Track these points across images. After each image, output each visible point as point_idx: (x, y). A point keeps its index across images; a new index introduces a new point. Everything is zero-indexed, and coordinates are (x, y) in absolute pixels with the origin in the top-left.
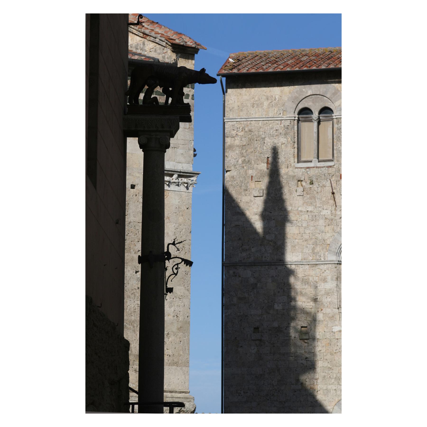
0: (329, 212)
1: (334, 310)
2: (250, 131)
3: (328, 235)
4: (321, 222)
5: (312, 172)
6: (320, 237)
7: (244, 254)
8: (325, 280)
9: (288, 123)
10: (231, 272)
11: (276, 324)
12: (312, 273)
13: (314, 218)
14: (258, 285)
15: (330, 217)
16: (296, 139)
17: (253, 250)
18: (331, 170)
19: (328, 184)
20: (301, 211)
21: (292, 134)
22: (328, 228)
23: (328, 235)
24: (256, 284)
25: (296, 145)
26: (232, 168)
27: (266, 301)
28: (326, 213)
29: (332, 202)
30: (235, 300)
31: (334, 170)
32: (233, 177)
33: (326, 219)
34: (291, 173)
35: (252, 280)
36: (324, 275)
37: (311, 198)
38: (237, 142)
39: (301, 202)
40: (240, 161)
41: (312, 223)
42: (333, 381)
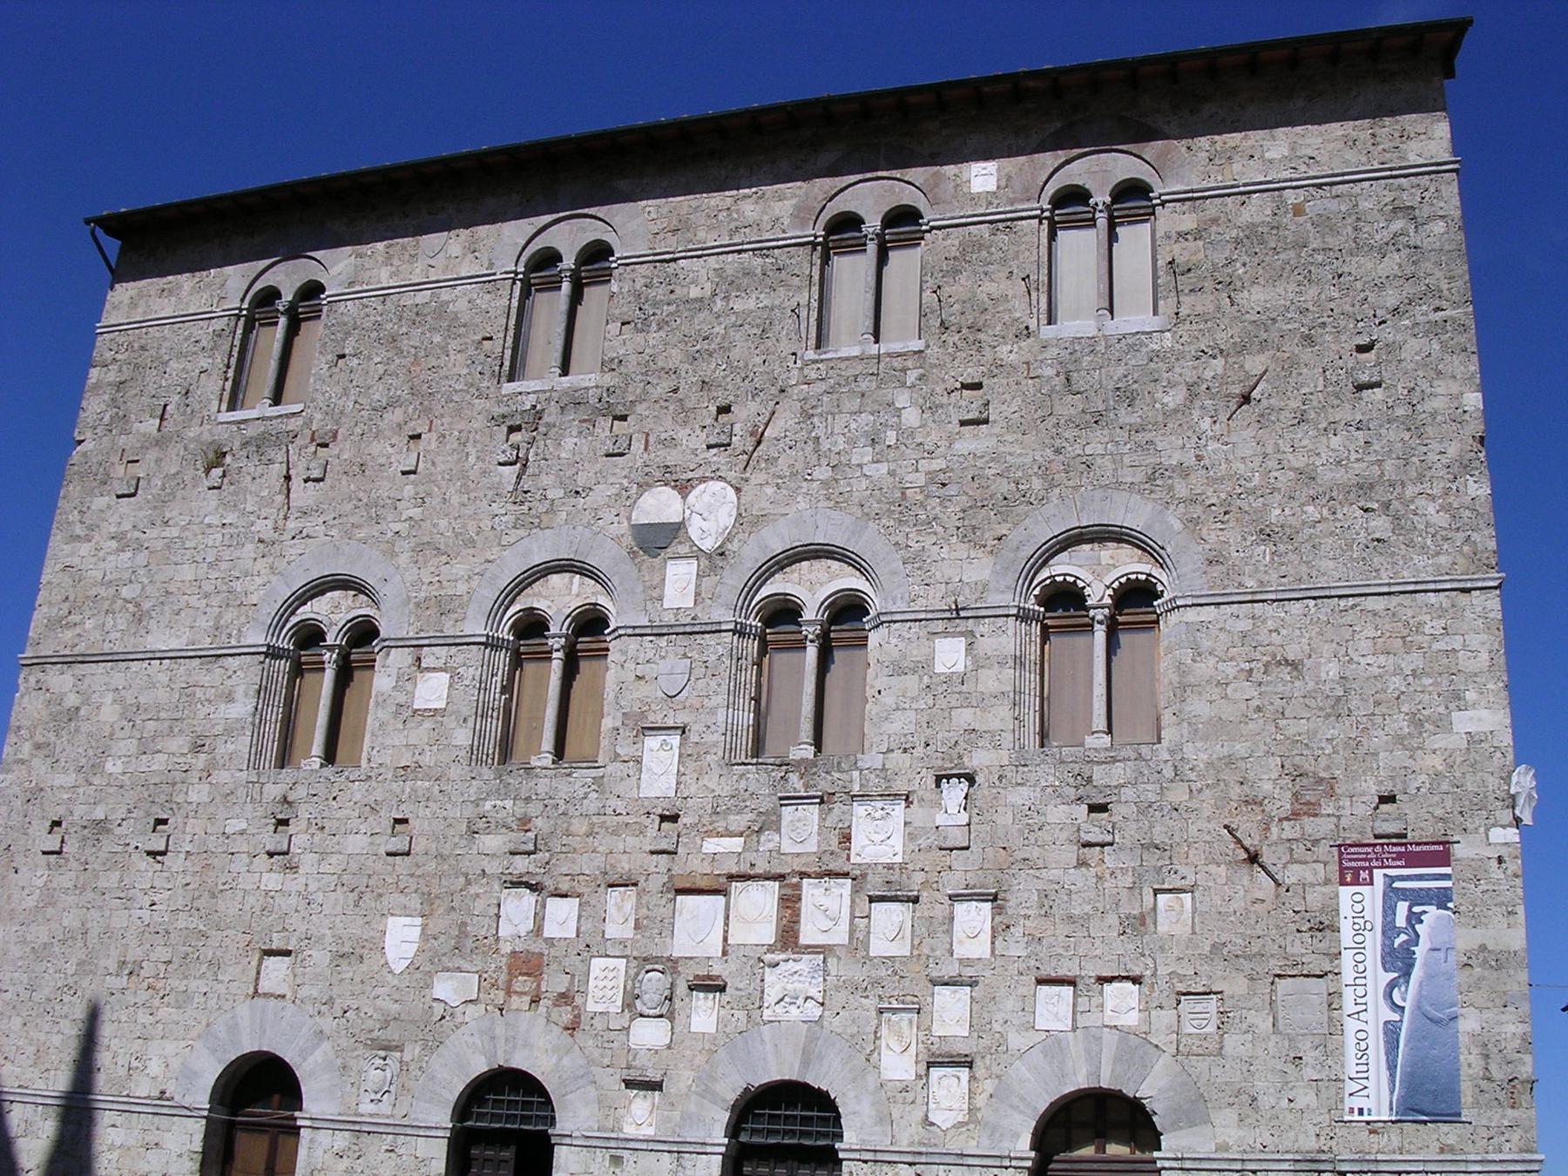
0: (270, 523)
1: (238, 774)
2: (143, 348)
3: (259, 581)
4: (249, 549)
5: (251, 431)
6: (238, 586)
7: (69, 635)
8: (230, 698)
9: (218, 325)
10: (32, 680)
11: (99, 813)
12: (205, 679)
13: (234, 541)
14: (82, 712)
15: (268, 535)
16: (233, 361)
17: (89, 625)
18: (294, 424)
19: (281, 457)
20: (209, 526)
21: (227, 347)
22: (261, 564)
23: (259, 581)
24: (78, 709)
25: (231, 374)
26: (89, 435)
27: (91, 752)
28: (264, 528)
29: (280, 498)
30: (27, 748)
31: (300, 421)
32: (85, 454)
33: (261, 541)
34: (207, 437)
35: (72, 700)
36: (229, 683)
37: (235, 493)
38: (112, 376)
39: (214, 503)
40: (107, 419)
41: (226, 555)
42: (204, 968)
